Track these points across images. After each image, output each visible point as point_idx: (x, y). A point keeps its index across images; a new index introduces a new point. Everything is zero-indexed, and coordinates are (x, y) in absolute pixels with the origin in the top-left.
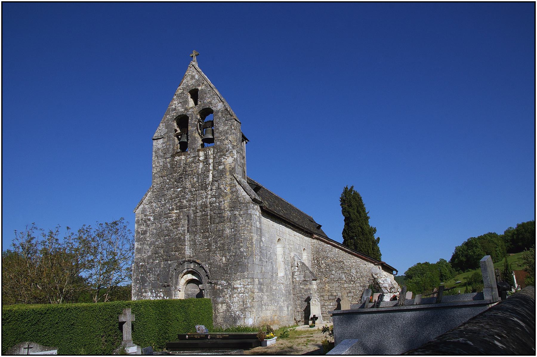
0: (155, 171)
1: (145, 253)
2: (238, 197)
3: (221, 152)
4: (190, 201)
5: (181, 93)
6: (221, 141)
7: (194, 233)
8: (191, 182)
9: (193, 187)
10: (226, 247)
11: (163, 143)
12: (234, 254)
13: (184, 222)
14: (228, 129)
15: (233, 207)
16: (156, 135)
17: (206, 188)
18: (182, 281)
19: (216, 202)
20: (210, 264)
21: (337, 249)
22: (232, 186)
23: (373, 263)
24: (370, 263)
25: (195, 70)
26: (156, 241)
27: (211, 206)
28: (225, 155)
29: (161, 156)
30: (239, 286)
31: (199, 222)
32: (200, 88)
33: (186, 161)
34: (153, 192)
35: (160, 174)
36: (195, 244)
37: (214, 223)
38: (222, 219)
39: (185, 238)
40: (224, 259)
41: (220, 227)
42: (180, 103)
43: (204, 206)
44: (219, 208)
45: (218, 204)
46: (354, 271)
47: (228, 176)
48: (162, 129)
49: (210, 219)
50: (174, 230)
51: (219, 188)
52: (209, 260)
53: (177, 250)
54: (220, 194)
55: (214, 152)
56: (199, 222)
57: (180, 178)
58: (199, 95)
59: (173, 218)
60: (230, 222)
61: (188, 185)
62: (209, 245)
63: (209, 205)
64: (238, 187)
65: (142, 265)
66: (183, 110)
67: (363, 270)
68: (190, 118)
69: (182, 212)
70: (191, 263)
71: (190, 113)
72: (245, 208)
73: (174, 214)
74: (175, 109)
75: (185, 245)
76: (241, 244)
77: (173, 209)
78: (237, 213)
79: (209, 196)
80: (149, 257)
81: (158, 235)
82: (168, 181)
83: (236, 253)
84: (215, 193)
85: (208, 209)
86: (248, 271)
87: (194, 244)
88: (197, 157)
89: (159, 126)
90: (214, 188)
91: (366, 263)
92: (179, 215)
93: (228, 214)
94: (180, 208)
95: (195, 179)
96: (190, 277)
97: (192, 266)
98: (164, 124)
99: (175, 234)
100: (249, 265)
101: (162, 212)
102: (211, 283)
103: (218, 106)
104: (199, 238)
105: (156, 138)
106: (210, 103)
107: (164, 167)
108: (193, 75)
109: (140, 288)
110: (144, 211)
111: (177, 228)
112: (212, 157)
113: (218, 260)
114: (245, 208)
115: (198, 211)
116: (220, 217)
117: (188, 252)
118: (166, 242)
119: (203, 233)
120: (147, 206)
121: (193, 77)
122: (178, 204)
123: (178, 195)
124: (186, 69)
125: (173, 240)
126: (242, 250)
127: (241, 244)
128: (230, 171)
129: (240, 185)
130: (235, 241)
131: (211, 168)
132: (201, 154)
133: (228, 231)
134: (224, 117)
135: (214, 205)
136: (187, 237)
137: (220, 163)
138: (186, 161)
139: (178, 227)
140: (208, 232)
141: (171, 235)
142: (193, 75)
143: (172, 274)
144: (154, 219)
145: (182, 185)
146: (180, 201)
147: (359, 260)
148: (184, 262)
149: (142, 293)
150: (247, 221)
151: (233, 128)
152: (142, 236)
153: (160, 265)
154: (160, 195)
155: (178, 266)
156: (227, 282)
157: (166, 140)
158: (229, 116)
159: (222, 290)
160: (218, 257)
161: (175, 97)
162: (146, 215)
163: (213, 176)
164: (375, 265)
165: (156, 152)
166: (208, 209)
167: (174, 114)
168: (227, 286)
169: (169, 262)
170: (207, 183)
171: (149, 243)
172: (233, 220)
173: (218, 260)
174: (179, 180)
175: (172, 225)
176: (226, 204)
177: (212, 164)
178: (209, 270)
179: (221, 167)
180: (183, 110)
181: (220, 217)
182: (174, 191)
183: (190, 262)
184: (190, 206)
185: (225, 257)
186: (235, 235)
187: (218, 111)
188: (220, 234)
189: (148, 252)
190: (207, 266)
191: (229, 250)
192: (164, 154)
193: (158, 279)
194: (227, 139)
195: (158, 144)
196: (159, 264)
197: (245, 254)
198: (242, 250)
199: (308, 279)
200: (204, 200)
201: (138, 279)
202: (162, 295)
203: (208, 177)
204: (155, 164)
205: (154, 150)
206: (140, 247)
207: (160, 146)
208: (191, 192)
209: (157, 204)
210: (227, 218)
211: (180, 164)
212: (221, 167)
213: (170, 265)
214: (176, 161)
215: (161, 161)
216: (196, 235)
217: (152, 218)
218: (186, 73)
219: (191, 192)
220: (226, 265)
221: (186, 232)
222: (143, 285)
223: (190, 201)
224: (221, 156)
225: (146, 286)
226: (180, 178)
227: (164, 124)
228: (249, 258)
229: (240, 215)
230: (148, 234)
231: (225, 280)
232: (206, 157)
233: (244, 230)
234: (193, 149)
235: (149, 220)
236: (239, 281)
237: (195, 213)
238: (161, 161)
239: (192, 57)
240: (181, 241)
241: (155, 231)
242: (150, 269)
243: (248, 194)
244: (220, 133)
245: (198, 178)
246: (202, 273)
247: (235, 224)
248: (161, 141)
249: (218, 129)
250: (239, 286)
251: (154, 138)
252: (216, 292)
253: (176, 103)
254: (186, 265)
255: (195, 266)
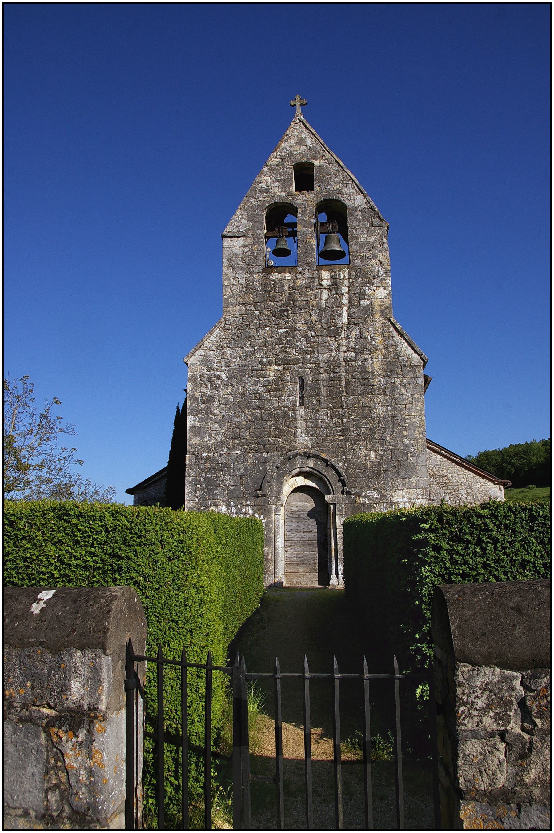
0: (227, 292)
1: (210, 435)
2: (398, 356)
3: (363, 277)
4: (306, 352)
5: (278, 165)
6: (364, 259)
7: (316, 408)
8: (305, 320)
9: (310, 329)
10: (377, 436)
11: (245, 246)
12: (391, 447)
13: (293, 387)
14: (375, 242)
15: (388, 372)
16: (229, 229)
17: (336, 335)
18: (287, 489)
19: (356, 359)
20: (347, 462)
21: (439, 456)
22: (386, 337)
23: (491, 481)
24: (487, 481)
25: (304, 129)
26: (235, 416)
27: (347, 365)
28: (373, 284)
29: (241, 268)
30: (402, 500)
31: (324, 390)
32: (316, 163)
33: (295, 283)
34: (225, 329)
35: (240, 299)
36: (316, 426)
37: (353, 395)
38: (369, 389)
39: (295, 414)
40: (373, 454)
41: (366, 401)
42: (277, 181)
43: (333, 365)
44: (363, 370)
45: (360, 363)
46: (463, 491)
47: (379, 320)
48: (239, 221)
49: (346, 387)
50: (273, 400)
51: (361, 336)
52: (344, 454)
53: (279, 433)
54: (364, 347)
55: (349, 274)
56: (324, 390)
57: (282, 311)
58: (315, 175)
59: (271, 379)
60: (385, 394)
61: (300, 324)
62: (345, 431)
63: (344, 364)
64: (398, 339)
65: (207, 458)
66: (283, 194)
67: (476, 491)
68: (300, 210)
69: (290, 369)
70: (309, 457)
71: (300, 201)
72: (412, 375)
73: (272, 372)
74: (267, 190)
75: (296, 427)
76: (405, 433)
77: (270, 363)
78: (397, 381)
79: (344, 349)
80: (219, 445)
81: (240, 406)
82: (257, 313)
83: (395, 446)
84: (355, 344)
85: (342, 370)
86: (417, 476)
87: (314, 428)
88: (317, 280)
89: (235, 214)
90: (352, 335)
91: (482, 480)
92: (283, 375)
93: (379, 381)
94: (286, 362)
95: (315, 317)
96: (301, 481)
97: (311, 463)
98: (245, 213)
99: (275, 405)
100: (420, 467)
101: (247, 365)
102: (349, 493)
103: (355, 200)
104: (323, 417)
105: (230, 234)
106: (340, 192)
107: (248, 288)
108: (299, 140)
109: (202, 498)
110: (205, 361)
111: (279, 397)
112: (346, 283)
113: (362, 455)
114: (412, 375)
115: (322, 371)
116: (364, 385)
117: (303, 440)
118: (256, 419)
119: (331, 408)
120: (212, 353)
121: (301, 142)
122: (281, 356)
123: (280, 339)
124: (287, 126)
125: (272, 416)
126: (407, 442)
127: (405, 433)
128: (382, 312)
129: (402, 336)
130: (393, 427)
131: (345, 300)
132: (325, 275)
133: (380, 410)
134: (367, 220)
135: (353, 363)
136: (301, 412)
137: (362, 296)
138: (295, 283)
139: (281, 395)
140: (342, 407)
141: (267, 407)
142: (299, 140)
143: (272, 477)
144: (230, 378)
145: (287, 323)
146: (284, 350)
147: (471, 475)
148: (295, 456)
149: (207, 507)
150: (416, 396)
151: (385, 240)
152: (203, 406)
153: (245, 459)
154: (240, 335)
155: (283, 463)
156: (380, 492)
157: (250, 241)
158: (377, 219)
159: (370, 505)
160: (362, 451)
161: (265, 169)
162: (209, 370)
163: (350, 316)
164: (495, 484)
165: (229, 260)
166: (342, 370)
167: (265, 198)
168: (380, 499)
169: (265, 455)
170: (339, 325)
171: (219, 418)
172: (390, 392)
173: (362, 455)
174: (281, 314)
175: (269, 391)
176: (375, 364)
177: (347, 296)
178: (346, 472)
179: (365, 303)
180: (283, 194)
181: (364, 385)
182: (272, 332)
183: (308, 456)
184: (304, 361)
185: (375, 451)
186: (393, 417)
187: (356, 209)
188: (366, 413)
189: (218, 434)
190: (341, 464)
191: (383, 441)
192: (248, 265)
193: (242, 484)
194: (375, 257)
195: (234, 247)
196: (244, 457)
197: (412, 448)
198: (406, 441)
199: (435, 498)
200: (333, 354)
201: (199, 482)
202: (251, 512)
203: (340, 315)
204: (228, 279)
205: (226, 254)
206: (198, 424)
207: (238, 250)
208: (306, 337)
209: (236, 352)
210: (379, 388)
211: (282, 286)
212: (365, 303)
213: (267, 460)
214: (274, 281)
215: (242, 278)
216: (318, 411)
217: (224, 376)
218: (288, 132)
219: (306, 337)
220: (378, 465)
221: (298, 404)
222: (210, 492)
223: (306, 352)
224: (364, 284)
225: (216, 495)
226: (282, 311)
227: (245, 213)
228: (418, 456)
229: (404, 386)
230: (217, 403)
231: (375, 490)
232: (335, 281)
233: (411, 410)
234: (308, 264)
235: (219, 378)
236: (401, 492)
237: (316, 373)
238: (242, 278)
239: (295, 105)
240: (288, 419)
241: (231, 399)
242: (224, 465)
243: (416, 352)
244: (362, 245)
245: (320, 315)
246: (331, 476)
247: (394, 398)
248: (240, 241)
249: (357, 238)
250: (402, 500)
251: (226, 234)
252: (359, 508)
253: (266, 179)
254: (298, 462)
255: (316, 464)
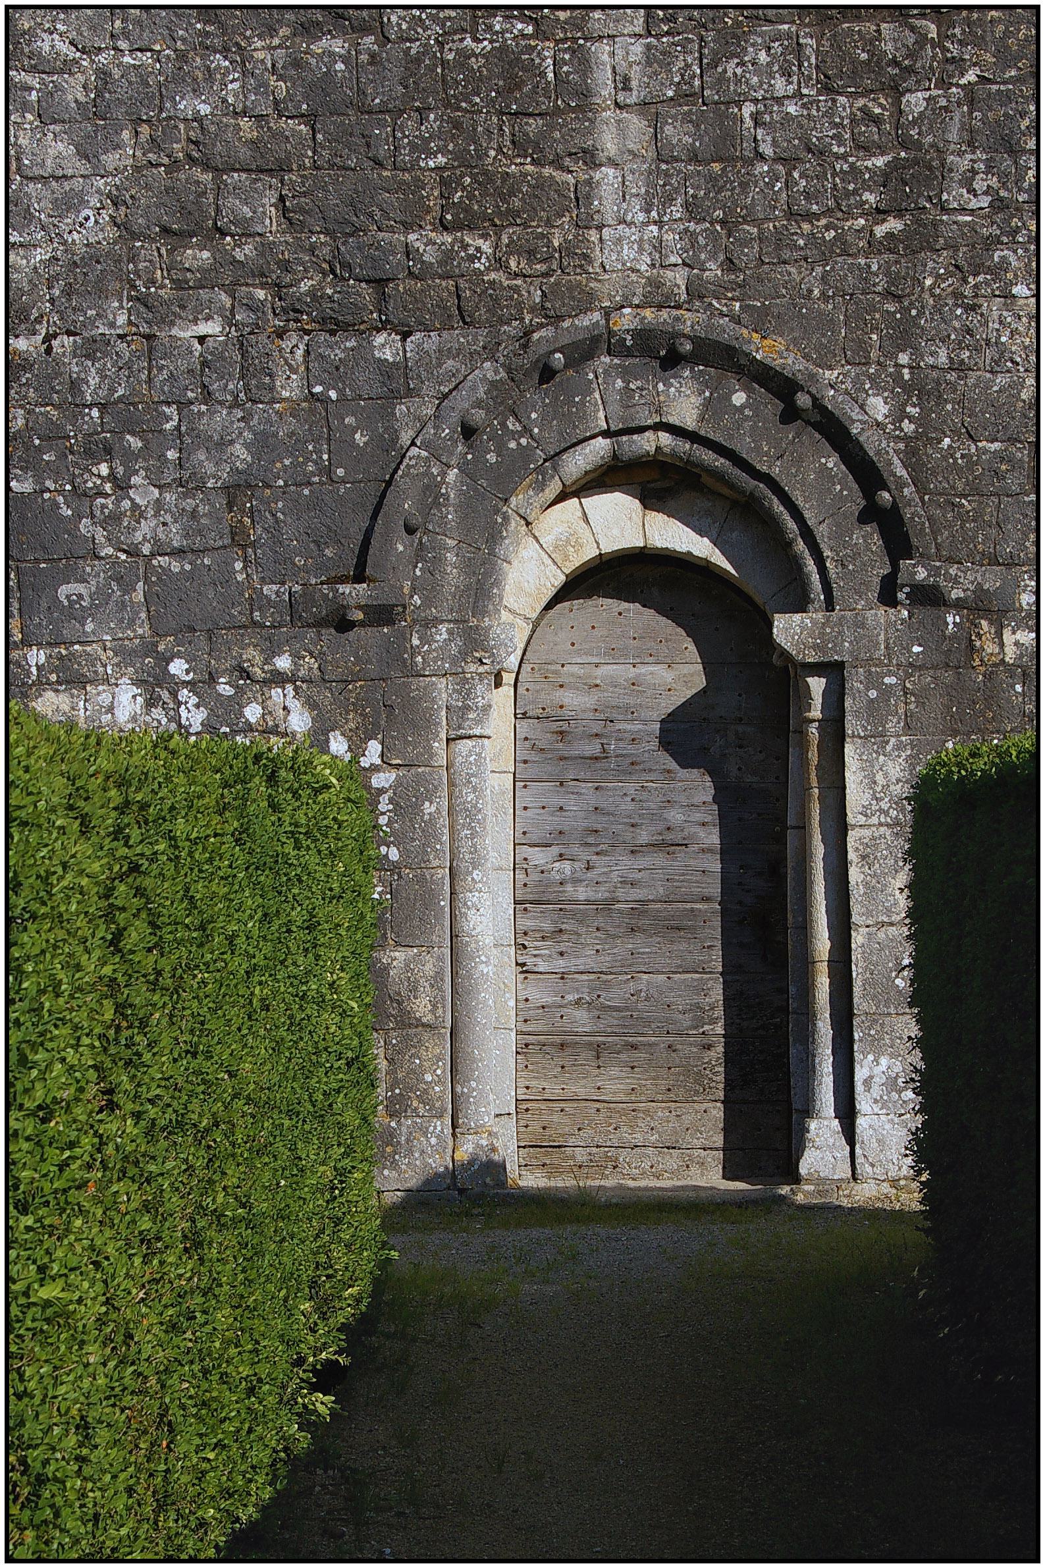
18: (529, 571)
20: (920, 389)
36: (725, 149)
39: (584, 63)
52: (904, 335)
62: (914, 178)
70: (672, 361)
75: (590, 158)
96: (618, 522)
97: (684, 402)
117: (631, 245)
143: (432, 493)
148: (583, 351)
155: (503, 400)
169: (386, 347)
171: (74, 90)
178: (912, 454)
183: (663, 354)
189: (69, 204)
190: (879, 407)
193: (238, 539)
202: (299, 721)
213: (397, 382)
225: (73, 612)
242: (125, 414)
246: (815, 484)
252: (992, 693)
254: (604, 393)
255: (713, 408)
